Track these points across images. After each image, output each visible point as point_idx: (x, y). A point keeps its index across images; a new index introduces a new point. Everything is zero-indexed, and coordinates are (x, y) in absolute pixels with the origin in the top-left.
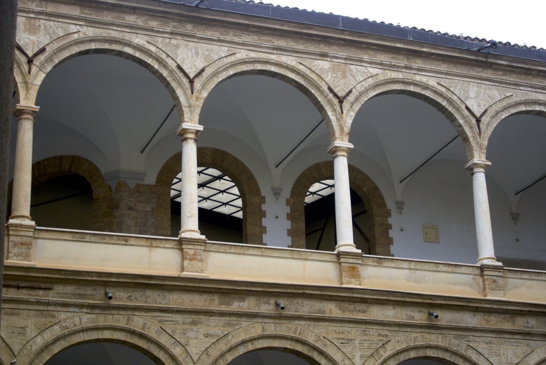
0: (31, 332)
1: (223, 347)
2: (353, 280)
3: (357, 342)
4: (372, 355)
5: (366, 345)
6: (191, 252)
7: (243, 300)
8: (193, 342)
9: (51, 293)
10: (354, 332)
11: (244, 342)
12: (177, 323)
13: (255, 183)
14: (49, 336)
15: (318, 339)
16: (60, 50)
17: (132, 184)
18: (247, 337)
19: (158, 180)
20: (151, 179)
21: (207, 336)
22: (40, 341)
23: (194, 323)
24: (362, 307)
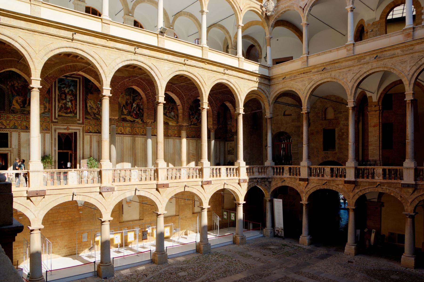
0: (307, 85)
1: (358, 75)
2: (408, 39)
3: (408, 62)
4: (415, 65)
5: (412, 62)
6: (349, 48)
7: (365, 59)
8: (349, 76)
9: (311, 73)
10: (406, 58)
11: (365, 73)
12: (344, 72)
13: (419, 3)
14: (311, 84)
15: (392, 64)
16: (311, 2)
17: (371, 23)
18: (366, 70)
19: (381, 18)
20: (378, 19)
21: (353, 74)
22: (309, 86)
23: (349, 70)
24: (412, 47)
